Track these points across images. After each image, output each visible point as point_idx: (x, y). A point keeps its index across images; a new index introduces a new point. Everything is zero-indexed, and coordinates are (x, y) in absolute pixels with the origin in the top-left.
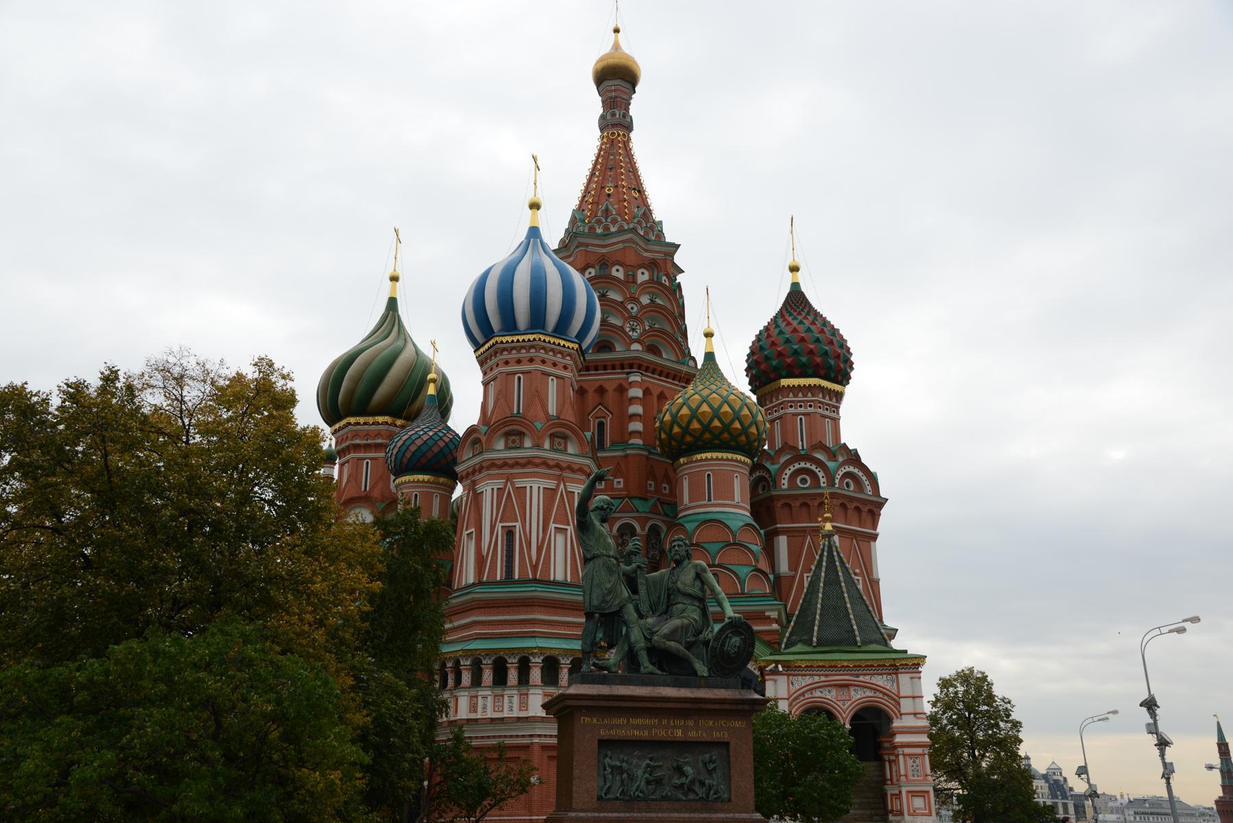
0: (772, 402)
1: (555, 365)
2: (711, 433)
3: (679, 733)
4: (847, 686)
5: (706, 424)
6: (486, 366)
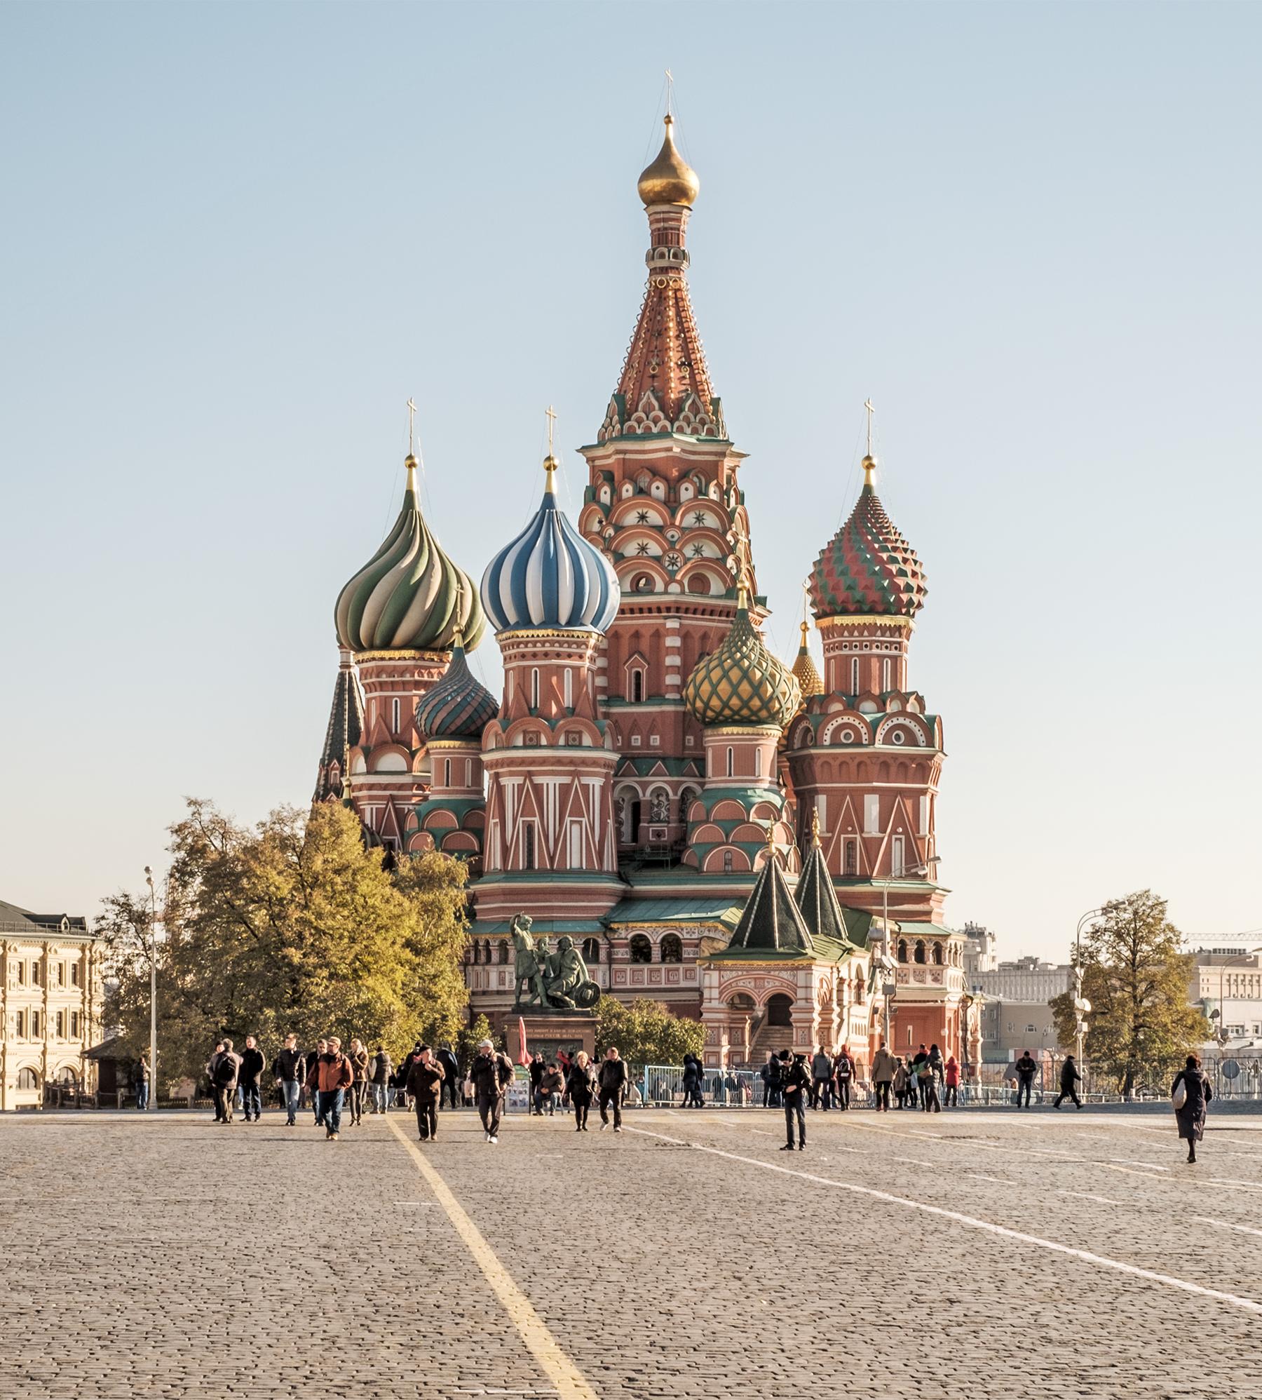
0: (829, 638)
1: (570, 656)
2: (731, 709)
3: (558, 1036)
5: (725, 700)
6: (506, 653)
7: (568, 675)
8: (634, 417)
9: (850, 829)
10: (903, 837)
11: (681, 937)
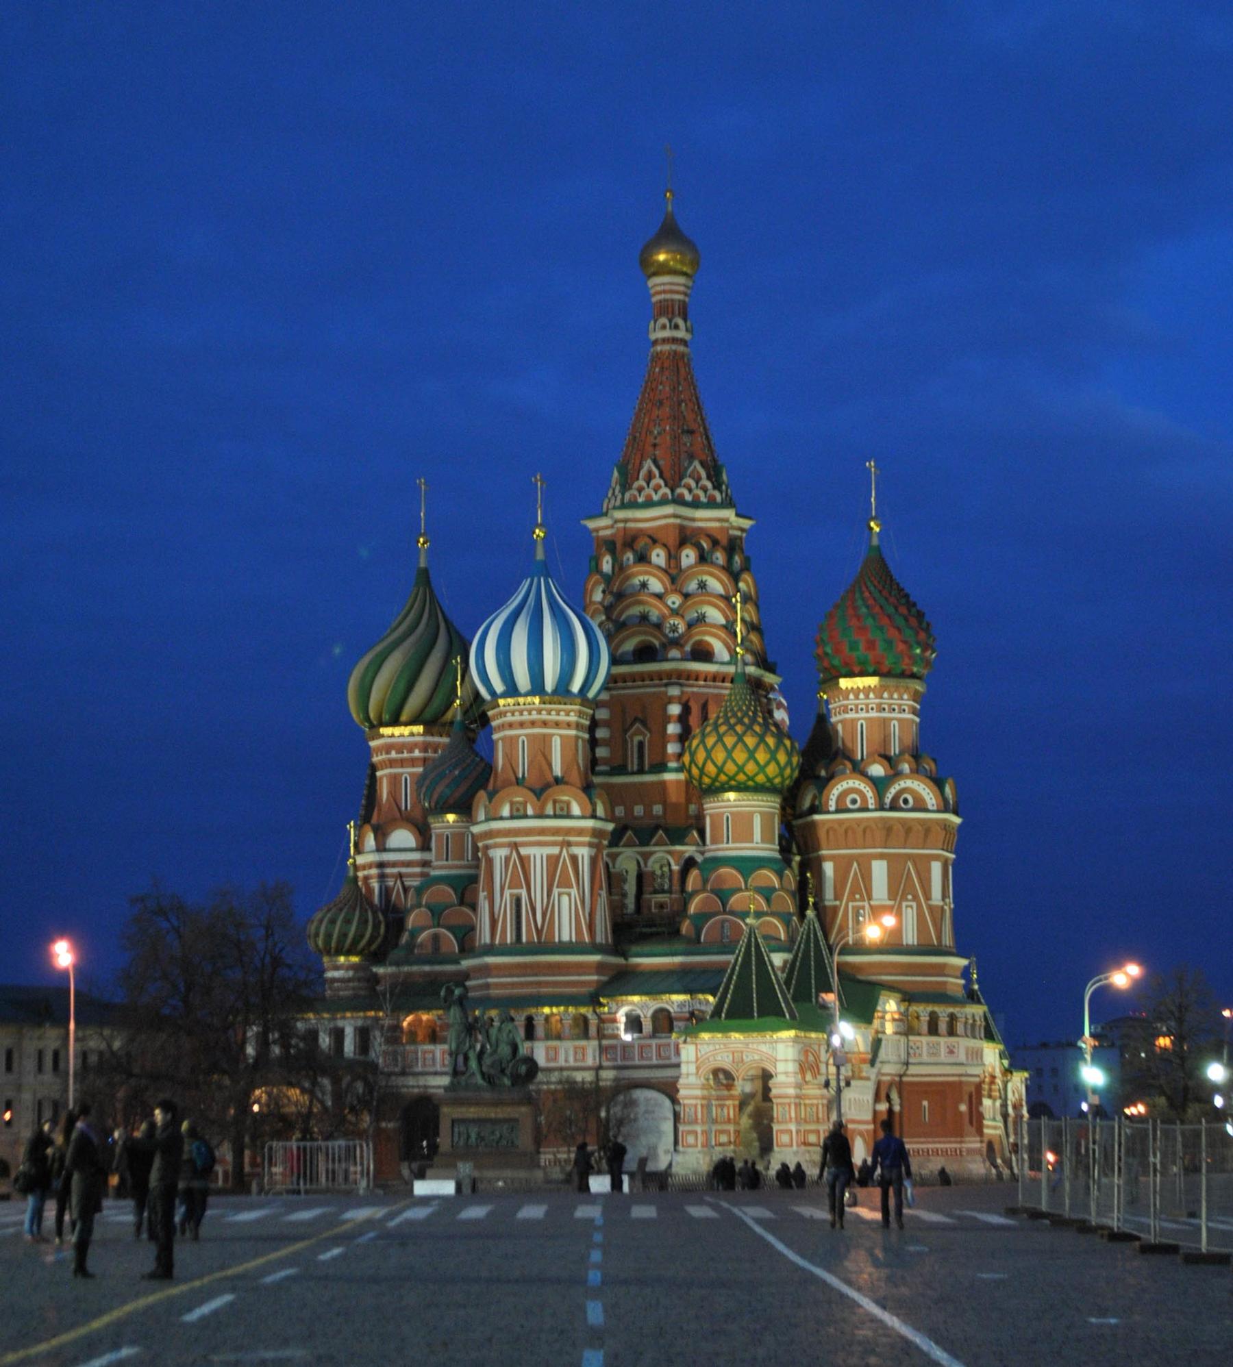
0: (835, 702)
1: (557, 725)
2: (727, 775)
3: (493, 1115)
4: (742, 1052)
7: (556, 744)
8: (636, 485)
9: (858, 896)
10: (914, 904)
11: (671, 1010)
